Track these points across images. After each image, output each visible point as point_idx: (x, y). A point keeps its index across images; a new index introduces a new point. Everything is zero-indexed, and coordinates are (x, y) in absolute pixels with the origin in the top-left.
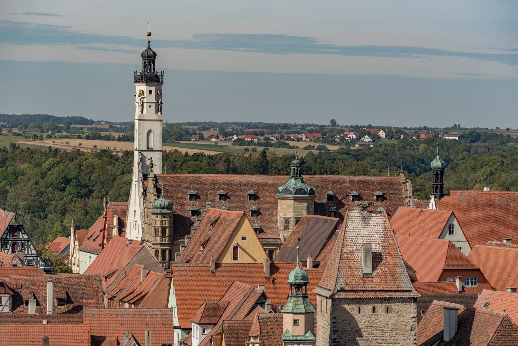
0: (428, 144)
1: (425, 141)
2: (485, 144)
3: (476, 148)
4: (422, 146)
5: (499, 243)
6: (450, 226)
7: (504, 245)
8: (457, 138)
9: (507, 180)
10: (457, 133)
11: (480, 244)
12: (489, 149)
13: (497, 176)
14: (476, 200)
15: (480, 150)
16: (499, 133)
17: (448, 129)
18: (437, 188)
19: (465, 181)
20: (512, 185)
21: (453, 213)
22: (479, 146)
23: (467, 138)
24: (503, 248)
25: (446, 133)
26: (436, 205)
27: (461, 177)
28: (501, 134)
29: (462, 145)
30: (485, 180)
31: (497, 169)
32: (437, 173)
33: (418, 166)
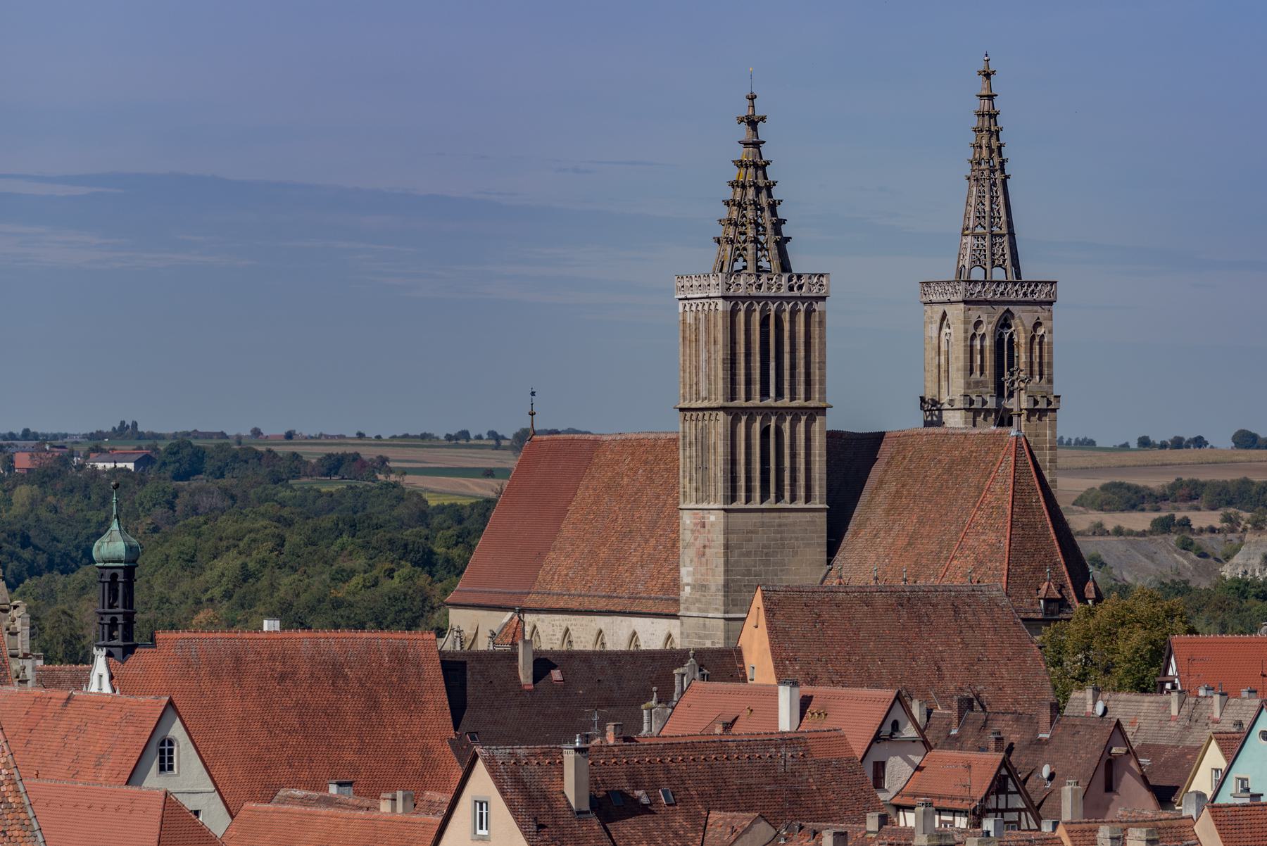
0: (42, 485)
1: (30, 477)
2: (222, 482)
3: (192, 494)
4: (22, 494)
5: (316, 794)
6: (163, 744)
7: (330, 802)
8: (131, 466)
9: (298, 595)
10: (129, 448)
11: (256, 800)
12: (233, 498)
13: (264, 582)
14: (238, 660)
15: (205, 502)
16: (262, 449)
17: (99, 436)
18: (113, 625)
19: (164, 600)
20: (312, 610)
21: (171, 703)
22: (201, 490)
23: (164, 464)
24: (332, 810)
25: (97, 450)
26: (111, 677)
27: (151, 588)
28: (269, 451)
29: (149, 488)
30: (228, 595)
31: (263, 563)
32: (114, 576)
33: (12, 555)
